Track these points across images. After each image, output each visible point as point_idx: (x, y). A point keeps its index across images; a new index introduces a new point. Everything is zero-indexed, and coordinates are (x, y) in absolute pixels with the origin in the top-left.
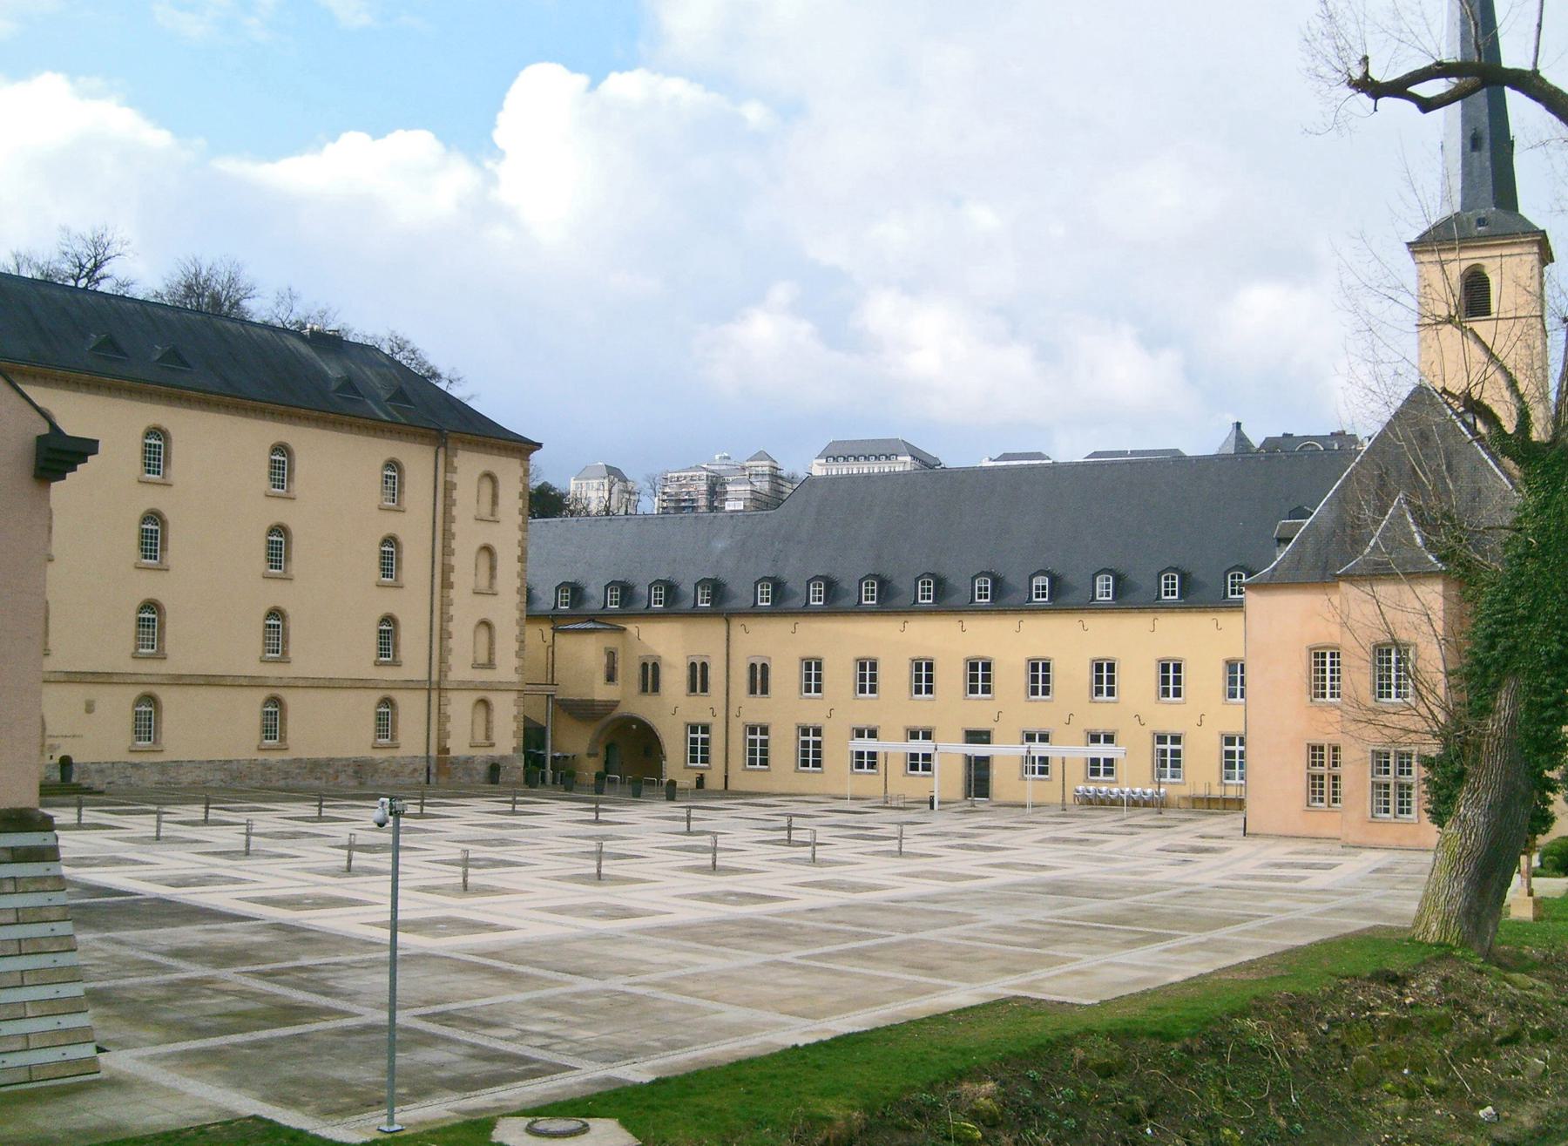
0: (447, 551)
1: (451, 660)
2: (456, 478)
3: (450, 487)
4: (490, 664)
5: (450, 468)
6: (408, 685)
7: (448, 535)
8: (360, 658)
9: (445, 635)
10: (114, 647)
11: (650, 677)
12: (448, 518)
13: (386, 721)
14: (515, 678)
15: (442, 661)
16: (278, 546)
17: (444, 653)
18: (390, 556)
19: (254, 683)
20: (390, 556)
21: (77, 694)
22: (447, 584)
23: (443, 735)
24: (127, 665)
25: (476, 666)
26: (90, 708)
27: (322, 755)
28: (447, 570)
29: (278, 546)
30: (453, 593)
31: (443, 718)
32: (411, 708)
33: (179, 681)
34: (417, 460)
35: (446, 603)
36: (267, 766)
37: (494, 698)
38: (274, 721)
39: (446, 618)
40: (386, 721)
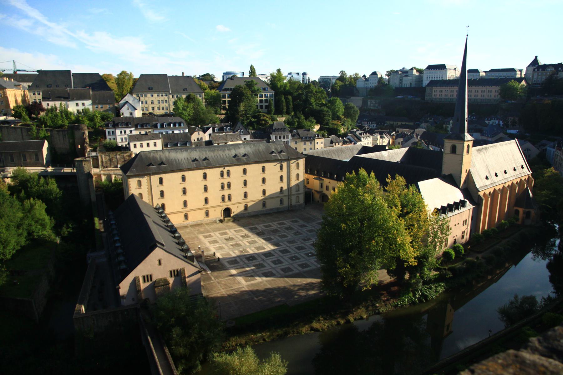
4: (299, 191)
6: (285, 196)
11: (327, 188)
13: (281, 202)
21: (236, 205)
23: (291, 202)
25: (297, 191)
27: (271, 208)
29: (264, 181)
36: (263, 211)
37: (300, 196)
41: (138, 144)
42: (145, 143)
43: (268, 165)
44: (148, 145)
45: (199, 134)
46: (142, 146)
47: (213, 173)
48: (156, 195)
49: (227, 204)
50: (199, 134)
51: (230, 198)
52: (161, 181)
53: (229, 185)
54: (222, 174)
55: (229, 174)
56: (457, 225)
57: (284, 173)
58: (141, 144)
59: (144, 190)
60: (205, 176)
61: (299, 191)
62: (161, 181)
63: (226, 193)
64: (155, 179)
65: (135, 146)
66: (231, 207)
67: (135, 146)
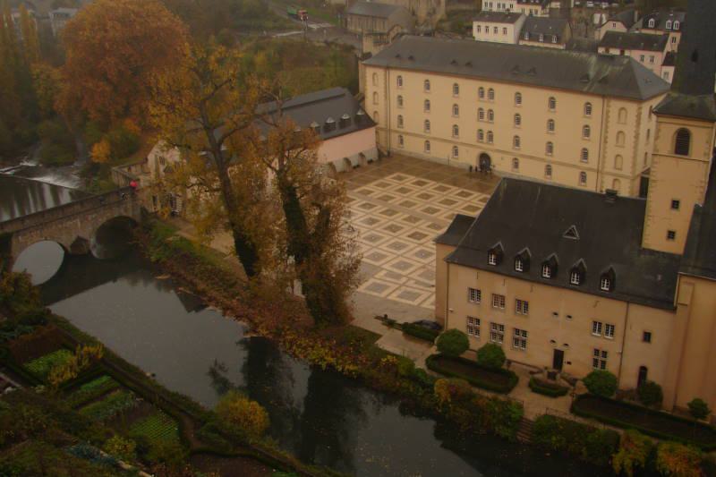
0: (606, 132)
1: (606, 165)
2: (611, 109)
3: (608, 112)
5: (608, 106)
7: (607, 127)
8: (575, 157)
9: (604, 157)
10: (509, 145)
12: (607, 122)
13: (583, 177)
14: (631, 175)
15: (603, 167)
16: (551, 125)
17: (604, 162)
18: (587, 131)
19: (543, 160)
20: (587, 131)
21: (500, 155)
22: (606, 142)
24: (511, 151)
25: (615, 168)
26: (502, 159)
28: (606, 138)
29: (551, 125)
30: (608, 145)
31: (602, 182)
32: (591, 177)
33: (523, 156)
34: (597, 103)
35: (605, 148)
38: (549, 171)
39: (605, 152)
40: (583, 177)
41: (483, 25)
42: (492, 26)
43: (561, 97)
44: (496, 30)
45: (614, 25)
46: (487, 30)
47: (469, 87)
48: (394, 102)
49: (485, 147)
50: (614, 25)
51: (491, 137)
52: (400, 82)
53: (491, 116)
54: (481, 93)
55: (492, 95)
56: (562, 317)
57: (594, 122)
58: (487, 27)
59: (381, 91)
60: (456, 89)
61: (621, 169)
62: (400, 82)
63: (486, 128)
64: (394, 74)
65: (479, 30)
66: (491, 154)
67: (479, 30)
